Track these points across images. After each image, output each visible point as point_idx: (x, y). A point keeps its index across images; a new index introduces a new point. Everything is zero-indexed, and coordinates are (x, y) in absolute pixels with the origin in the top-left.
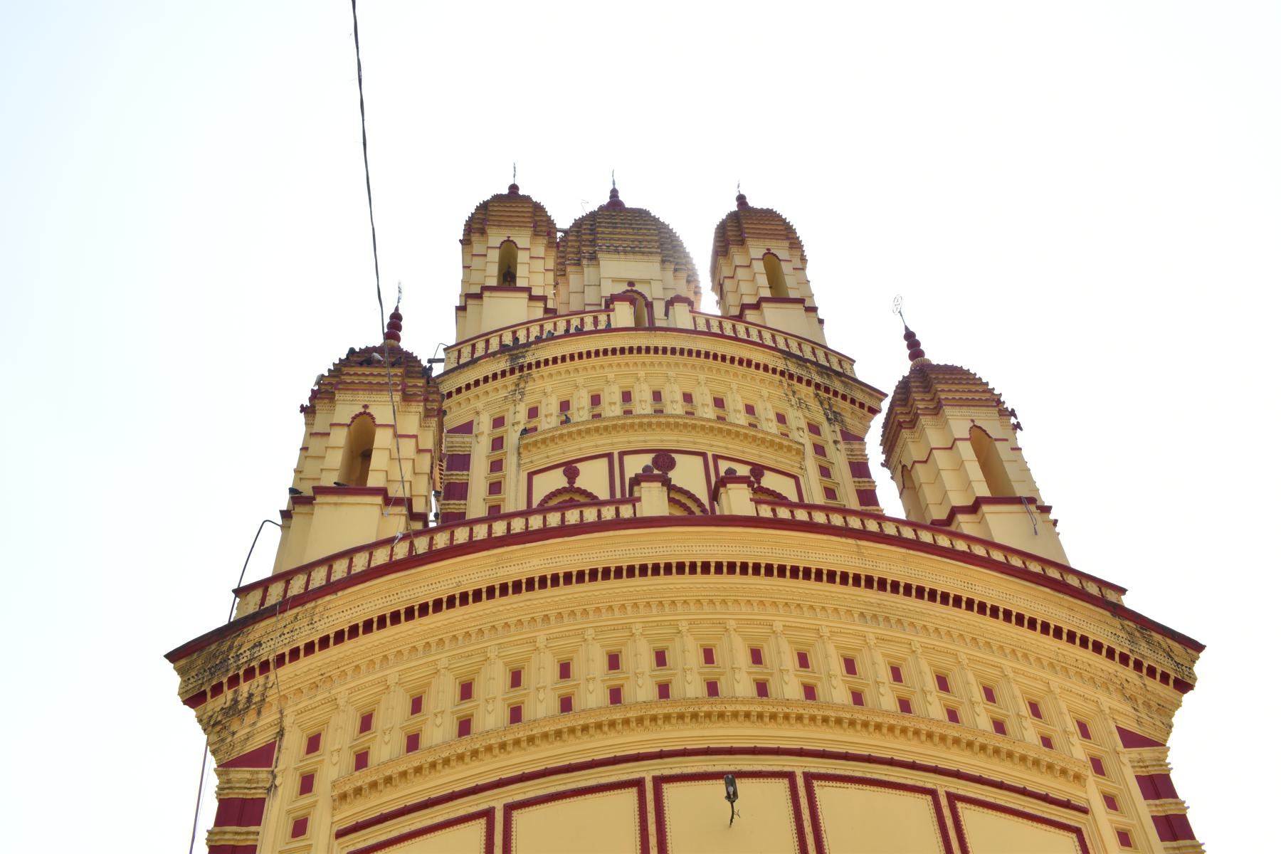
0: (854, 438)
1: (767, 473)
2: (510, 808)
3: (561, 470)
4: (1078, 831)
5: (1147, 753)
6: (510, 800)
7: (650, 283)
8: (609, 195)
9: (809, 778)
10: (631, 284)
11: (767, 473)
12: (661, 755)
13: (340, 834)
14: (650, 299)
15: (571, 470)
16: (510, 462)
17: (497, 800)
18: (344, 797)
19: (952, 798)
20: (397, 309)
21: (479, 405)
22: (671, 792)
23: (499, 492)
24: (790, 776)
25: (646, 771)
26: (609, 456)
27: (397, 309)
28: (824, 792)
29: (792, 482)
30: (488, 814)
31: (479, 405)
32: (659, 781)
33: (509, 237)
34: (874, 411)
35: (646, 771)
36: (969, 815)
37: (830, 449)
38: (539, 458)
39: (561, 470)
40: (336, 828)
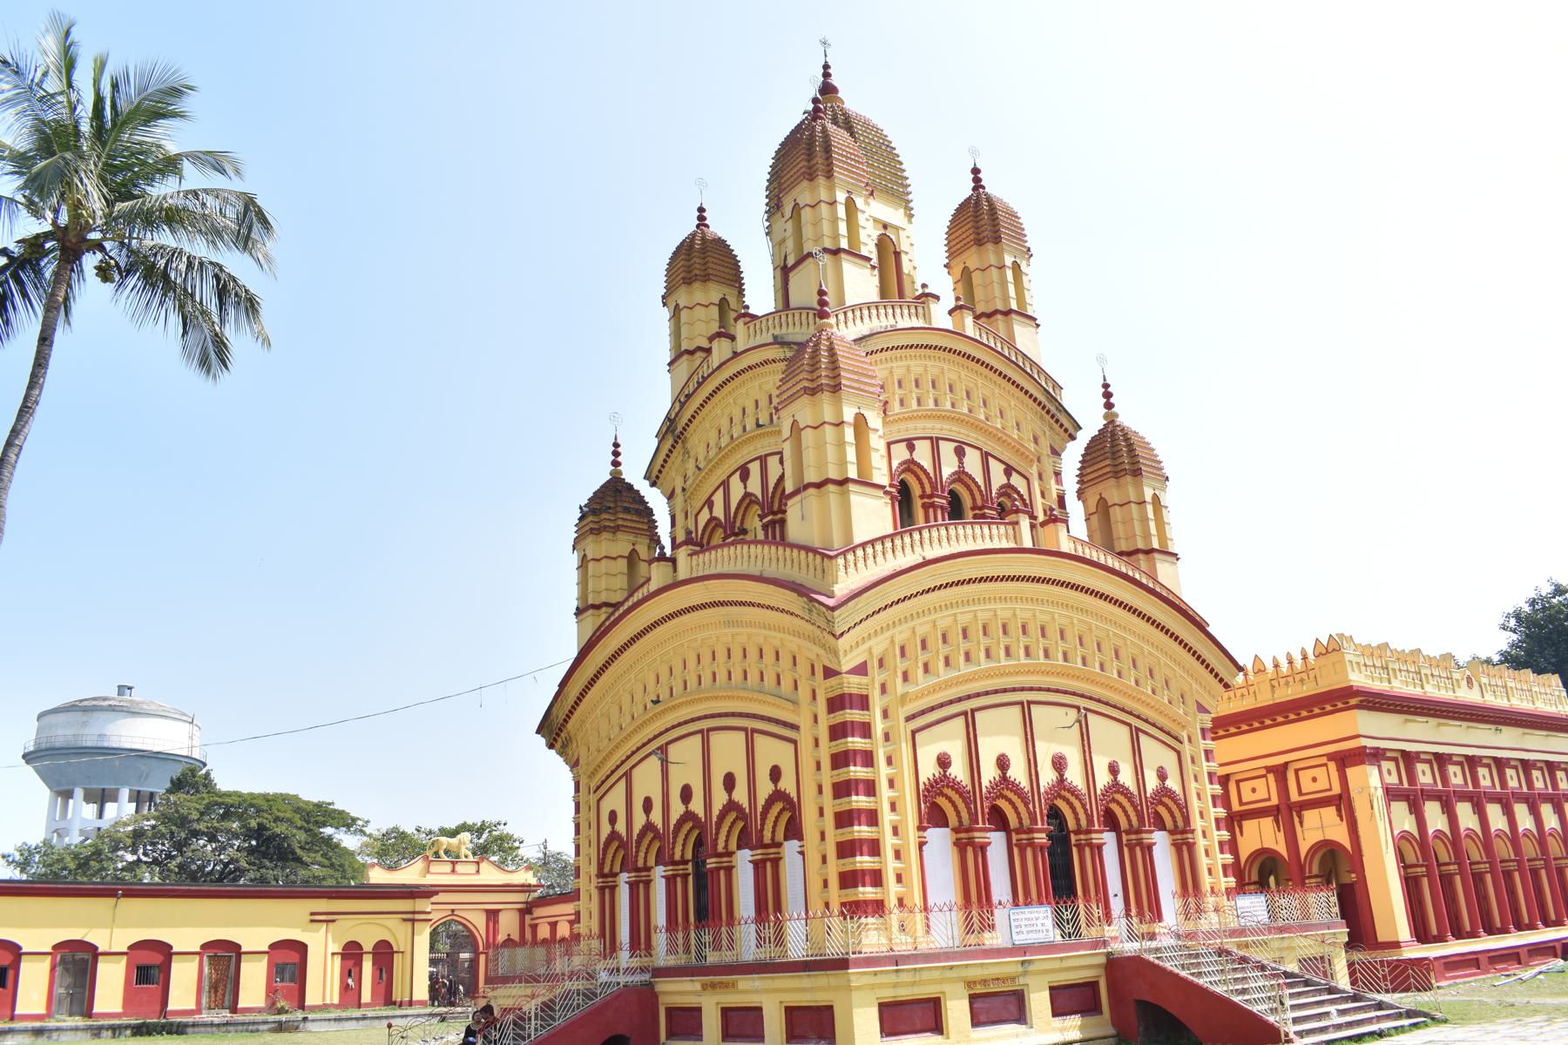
0: (1056, 453)
1: (1014, 474)
3: (904, 444)
4: (1179, 753)
6: (974, 706)
10: (885, 226)
11: (1014, 474)
12: (1031, 689)
13: (909, 719)
15: (911, 448)
19: (1138, 729)
24: (1078, 708)
25: (1025, 696)
28: (1090, 716)
29: (1025, 481)
30: (965, 713)
34: (1073, 438)
35: (1025, 696)
36: (1143, 738)
37: (1044, 459)
39: (904, 444)
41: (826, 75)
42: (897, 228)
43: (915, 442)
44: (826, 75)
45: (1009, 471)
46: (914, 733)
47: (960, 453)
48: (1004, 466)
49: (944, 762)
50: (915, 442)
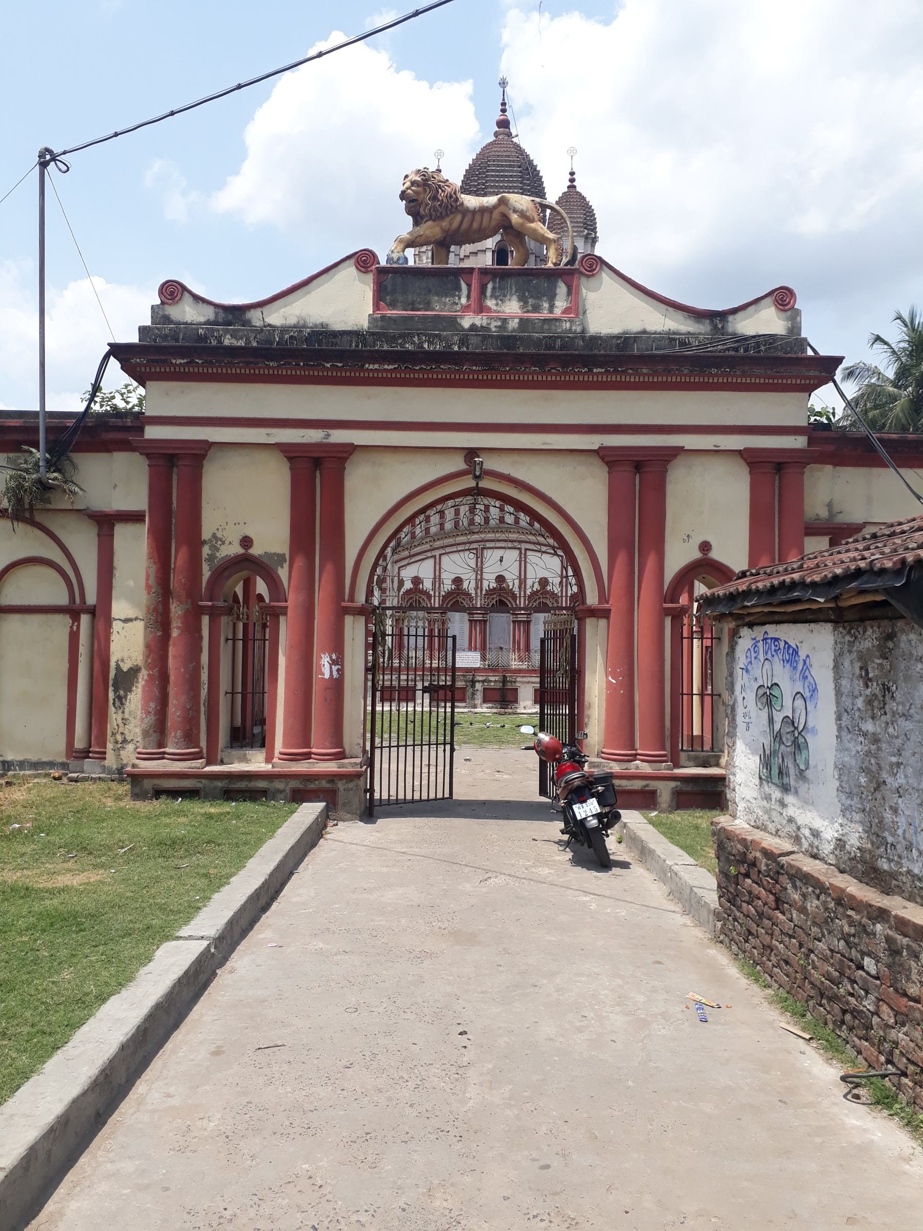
9: (526, 550)
17: (437, 553)
28: (529, 553)
46: (399, 568)
49: (417, 581)
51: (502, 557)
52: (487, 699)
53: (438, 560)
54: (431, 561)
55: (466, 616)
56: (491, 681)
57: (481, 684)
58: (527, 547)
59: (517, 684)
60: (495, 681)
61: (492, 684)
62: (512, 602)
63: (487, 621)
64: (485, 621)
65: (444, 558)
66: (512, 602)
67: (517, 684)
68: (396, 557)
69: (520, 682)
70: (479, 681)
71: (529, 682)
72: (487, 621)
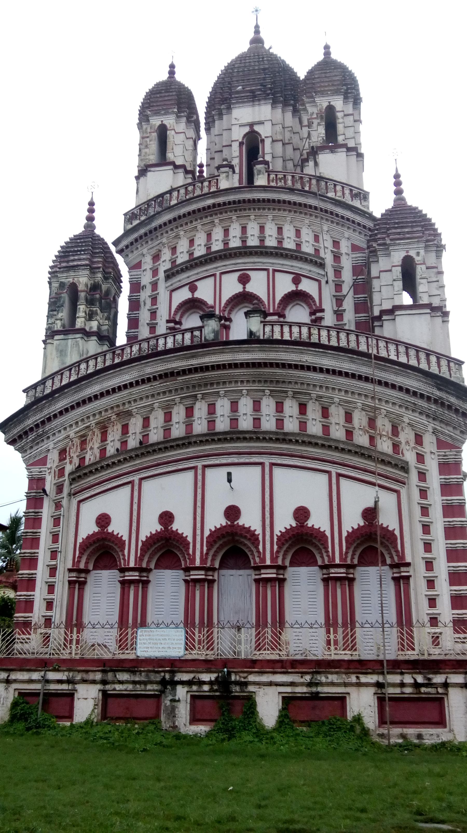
1: (303, 279)
2: (141, 479)
3: (188, 286)
5: (450, 453)
7: (263, 123)
8: (254, 30)
9: (272, 465)
11: (303, 279)
14: (263, 137)
15: (193, 288)
16: (162, 285)
17: (136, 478)
18: (74, 479)
20: (92, 198)
21: (145, 251)
22: (209, 472)
23: (156, 304)
24: (262, 464)
25: (199, 464)
26: (214, 275)
27: (92, 198)
28: (277, 471)
30: (131, 482)
31: (145, 251)
32: (205, 467)
33: (162, 121)
38: (176, 281)
40: (72, 491)
41: (257, 31)
42: (261, 123)
43: (196, 283)
44: (257, 31)
45: (297, 280)
47: (244, 280)
48: (292, 276)
50: (196, 283)
51: (229, 474)
52: (198, 717)
53: (136, 488)
54: (128, 489)
55: (180, 574)
56: (204, 683)
57: (186, 689)
58: (274, 461)
59: (251, 688)
60: (211, 683)
61: (206, 688)
62: (253, 548)
63: (213, 581)
64: (211, 582)
65: (145, 484)
66: (253, 548)
67: (251, 688)
68: (77, 486)
69: (255, 683)
70: (182, 683)
71: (271, 684)
72: (213, 581)
